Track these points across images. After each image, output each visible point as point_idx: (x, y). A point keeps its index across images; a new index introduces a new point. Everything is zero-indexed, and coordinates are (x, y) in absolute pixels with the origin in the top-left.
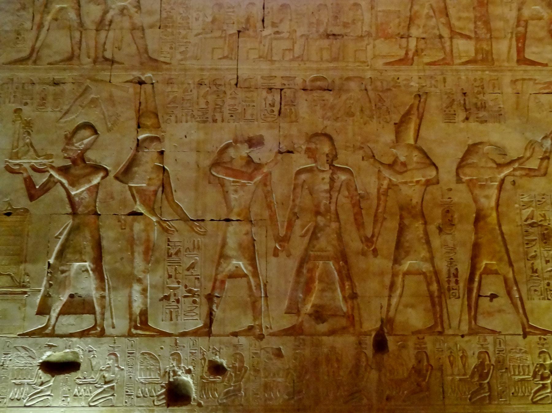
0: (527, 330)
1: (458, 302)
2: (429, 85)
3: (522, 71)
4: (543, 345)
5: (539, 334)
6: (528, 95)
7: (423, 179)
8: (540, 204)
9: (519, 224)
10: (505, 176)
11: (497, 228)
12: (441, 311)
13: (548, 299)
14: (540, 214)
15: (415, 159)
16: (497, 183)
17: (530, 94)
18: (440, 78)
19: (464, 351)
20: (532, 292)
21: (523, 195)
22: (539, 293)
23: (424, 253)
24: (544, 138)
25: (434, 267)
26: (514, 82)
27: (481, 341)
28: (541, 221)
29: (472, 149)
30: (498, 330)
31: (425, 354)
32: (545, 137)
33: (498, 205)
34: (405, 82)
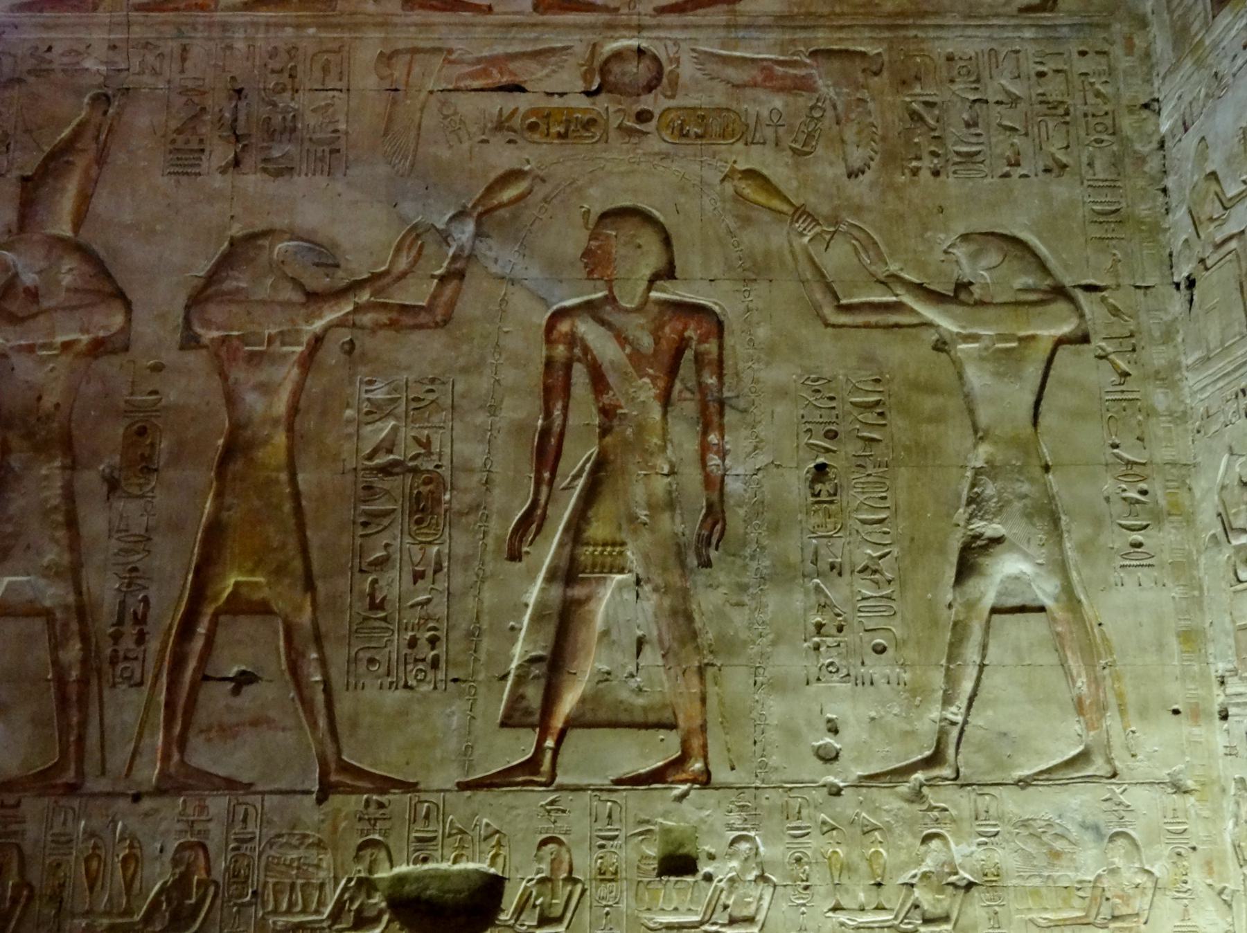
0: (334, 778)
1: (138, 698)
2: (136, 68)
4: (373, 821)
5: (368, 791)
6: (423, 95)
7: (85, 338)
8: (419, 408)
9: (349, 466)
10: (326, 329)
11: (284, 477)
12: (83, 724)
13: (406, 686)
14: (415, 438)
15: (67, 280)
16: (299, 349)
17: (431, 92)
18: (173, 46)
19: (134, 842)
20: (362, 668)
21: (371, 382)
22: (383, 670)
23: (52, 555)
24: (452, 219)
25: (79, 593)
26: (387, 58)
27: (190, 811)
29: (239, 251)
30: (245, 778)
31: (15, 852)
32: (460, 215)
33: (294, 409)
34: (65, 60)
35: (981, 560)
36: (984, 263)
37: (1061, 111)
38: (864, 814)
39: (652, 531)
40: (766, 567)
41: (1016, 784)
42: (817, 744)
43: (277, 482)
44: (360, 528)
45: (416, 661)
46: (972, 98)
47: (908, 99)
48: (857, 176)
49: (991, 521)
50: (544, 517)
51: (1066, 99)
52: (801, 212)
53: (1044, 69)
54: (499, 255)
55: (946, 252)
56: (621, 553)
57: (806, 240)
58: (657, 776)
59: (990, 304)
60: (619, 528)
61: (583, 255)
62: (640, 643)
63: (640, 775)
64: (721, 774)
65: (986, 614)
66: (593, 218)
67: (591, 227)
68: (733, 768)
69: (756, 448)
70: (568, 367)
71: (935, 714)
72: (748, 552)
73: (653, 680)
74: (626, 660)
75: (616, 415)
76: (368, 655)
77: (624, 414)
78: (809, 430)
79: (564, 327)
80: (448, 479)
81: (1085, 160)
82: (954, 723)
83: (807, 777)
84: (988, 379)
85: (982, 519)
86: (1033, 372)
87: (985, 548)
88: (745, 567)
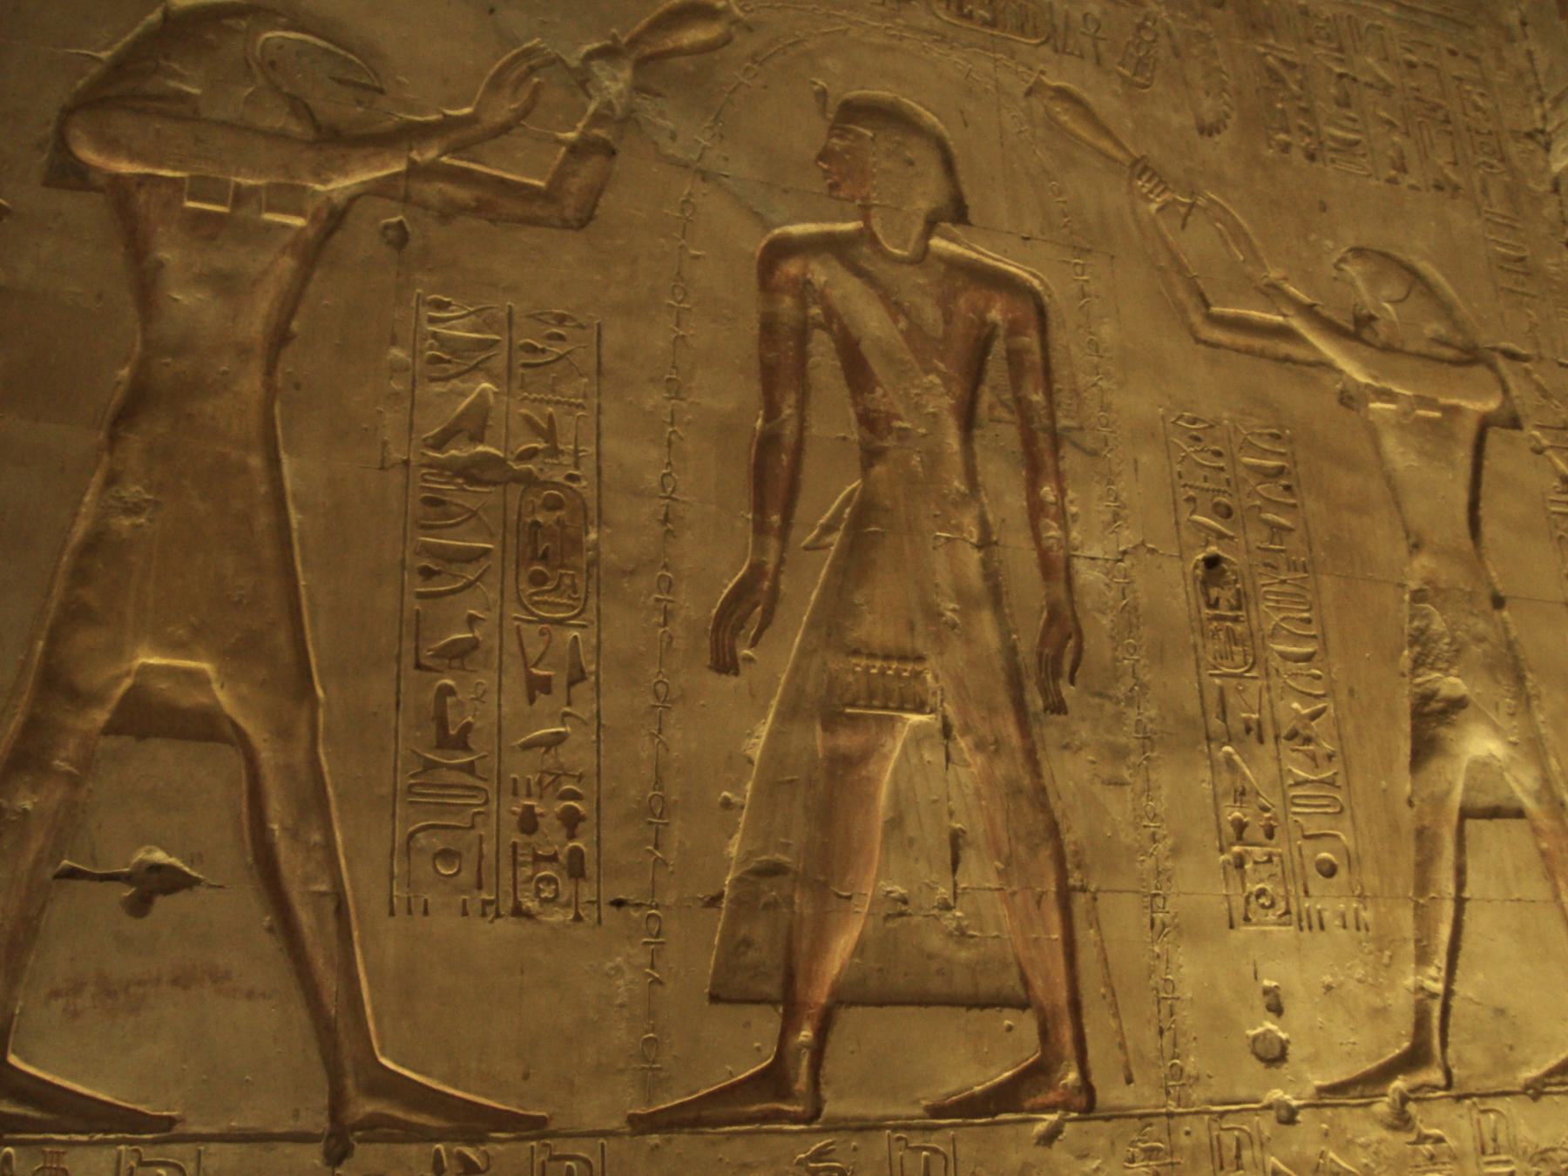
9: (397, 456)
11: (256, 461)
13: (518, 911)
14: (528, 420)
21: (441, 306)
22: (467, 876)
28: (530, 454)
33: (280, 338)
35: (1443, 731)
36: (1386, 291)
37: (1440, 115)
38: (1332, 1155)
39: (969, 641)
40: (1152, 720)
41: (1524, 1091)
42: (1251, 1033)
43: (244, 469)
44: (419, 579)
45: (537, 859)
46: (1338, 70)
47: (1262, 50)
48: (1210, 135)
49: (1446, 672)
50: (775, 590)
51: (1443, 103)
52: (1141, 167)
53: (1414, 58)
54: (675, 126)
55: (1336, 266)
56: (917, 675)
57: (1154, 207)
58: (1004, 1098)
59: (1401, 351)
60: (911, 627)
61: (821, 157)
62: (956, 841)
63: (973, 1097)
64: (1112, 1094)
65: (1455, 818)
66: (833, 106)
67: (831, 116)
68: (1129, 1081)
69: (1116, 516)
70: (802, 334)
71: (1410, 981)
72: (1121, 690)
73: (988, 913)
74: (935, 877)
75: (890, 430)
76: (438, 843)
77: (905, 429)
78: (1191, 500)
79: (792, 268)
80: (592, 504)
81: (1477, 185)
82: (1433, 995)
83: (1242, 1092)
84: (1412, 460)
85: (1433, 668)
86: (1463, 456)
87: (1443, 713)
88: (1119, 718)
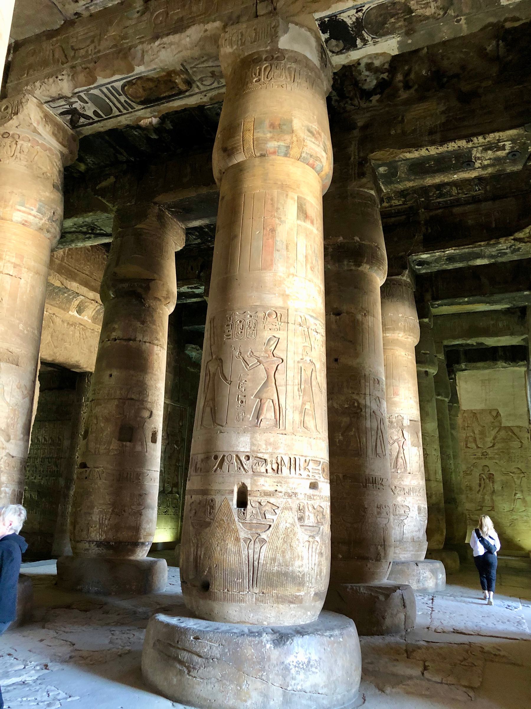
3: (468, 450)
54: (475, 469)
